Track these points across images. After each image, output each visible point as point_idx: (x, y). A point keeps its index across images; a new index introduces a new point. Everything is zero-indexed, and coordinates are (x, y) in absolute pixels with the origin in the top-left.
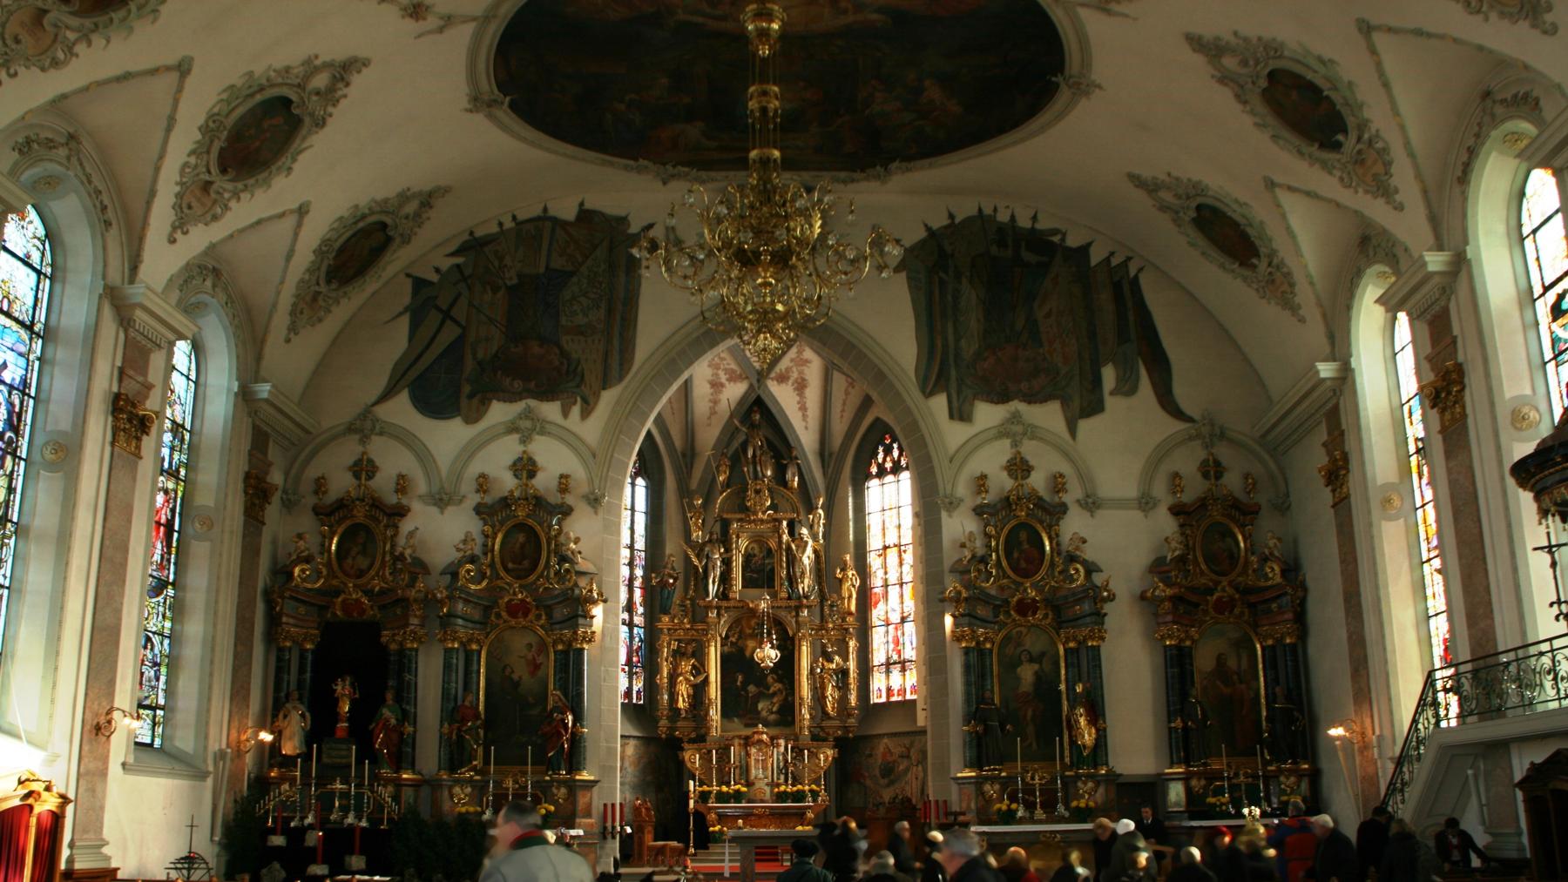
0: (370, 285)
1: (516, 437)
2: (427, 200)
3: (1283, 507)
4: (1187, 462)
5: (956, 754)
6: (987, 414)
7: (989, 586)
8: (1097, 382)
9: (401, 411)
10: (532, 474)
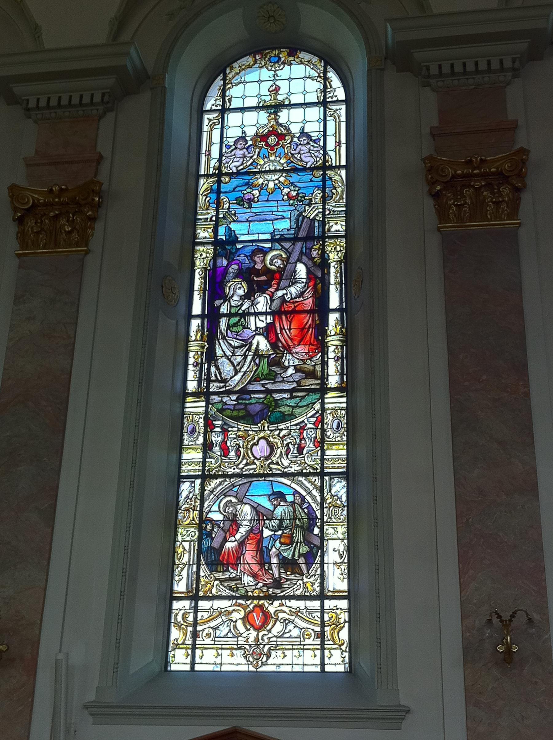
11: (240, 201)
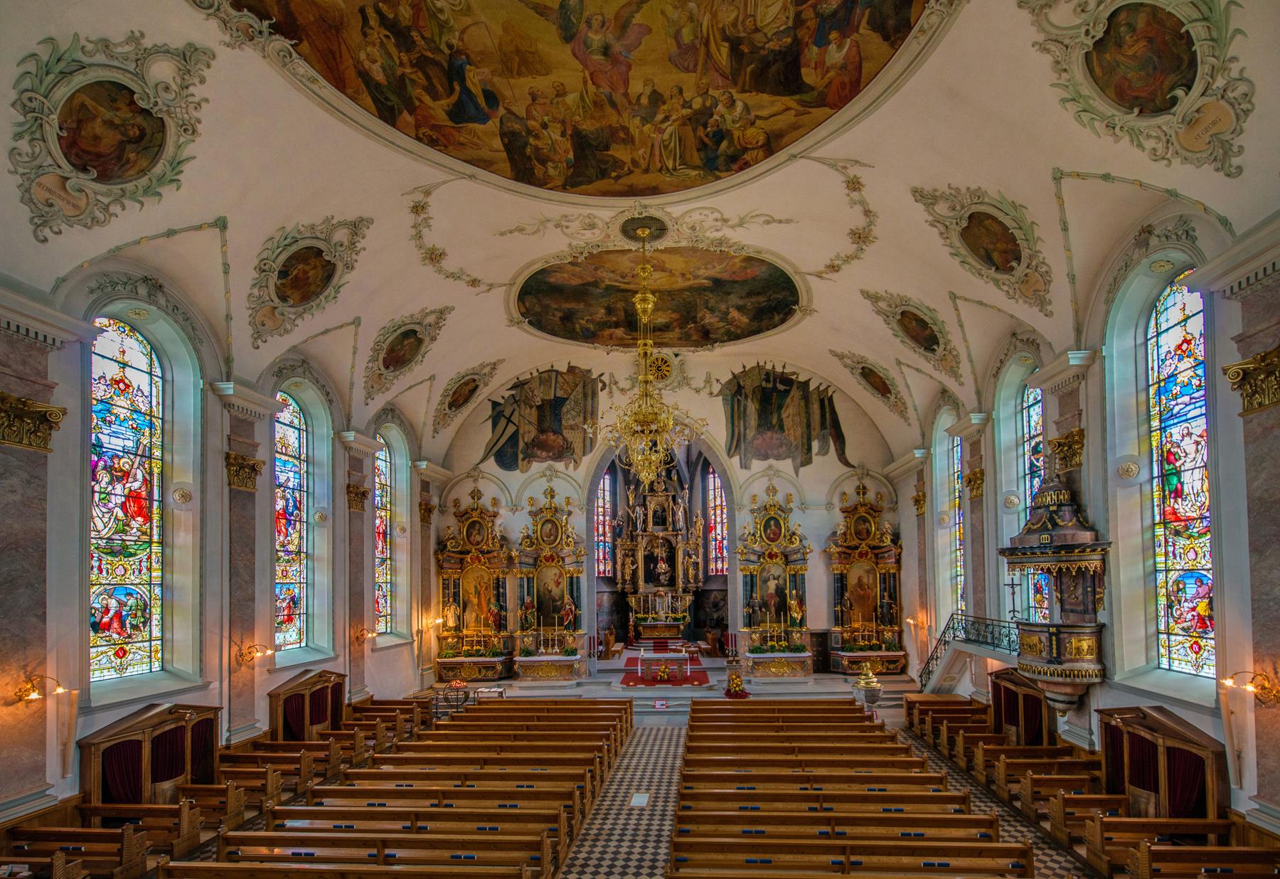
0: (471, 406)
1: (544, 479)
2: (494, 366)
3: (894, 510)
4: (850, 488)
5: (740, 621)
6: (757, 465)
7: (756, 547)
8: (809, 449)
9: (491, 465)
10: (552, 497)
11: (104, 420)
